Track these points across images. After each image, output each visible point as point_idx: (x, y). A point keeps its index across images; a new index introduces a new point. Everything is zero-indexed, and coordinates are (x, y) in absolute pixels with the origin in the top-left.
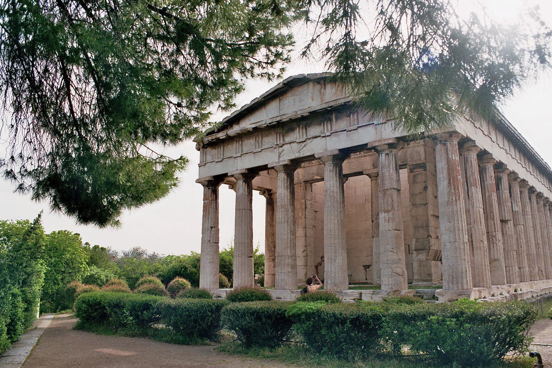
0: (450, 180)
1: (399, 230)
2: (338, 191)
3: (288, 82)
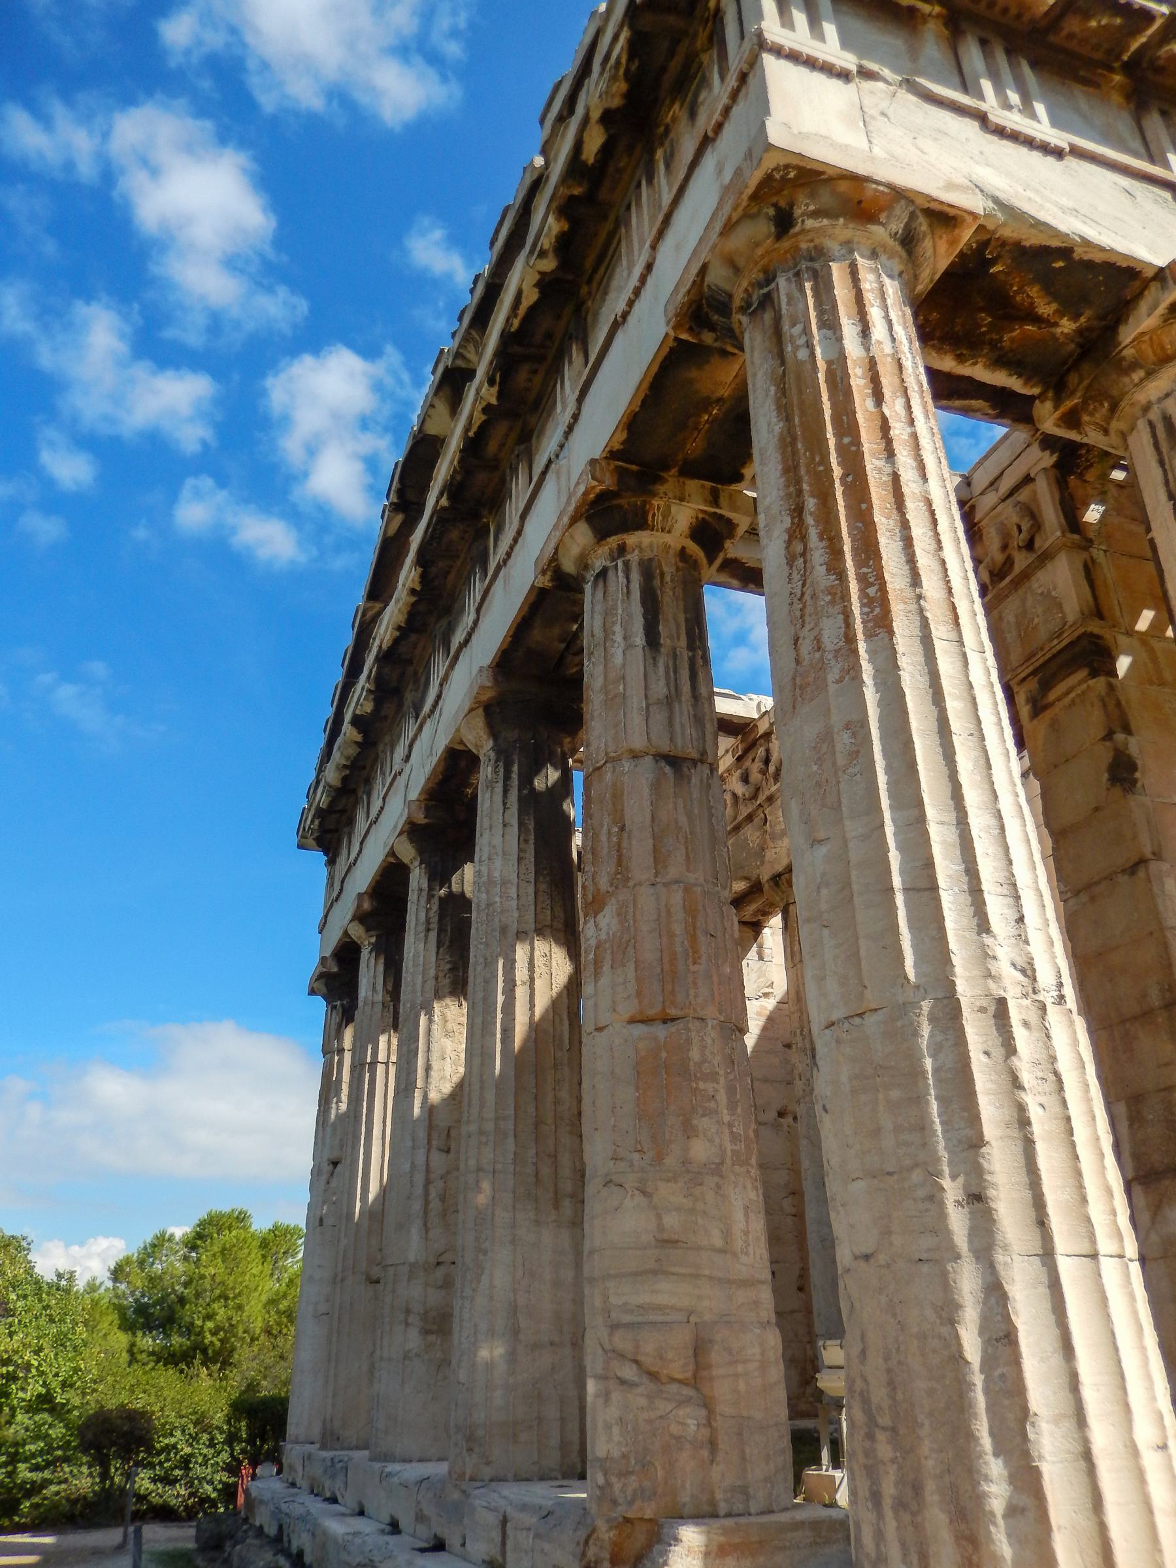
0: (798, 511)
1: (667, 1020)
2: (514, 877)
3: (401, 493)
